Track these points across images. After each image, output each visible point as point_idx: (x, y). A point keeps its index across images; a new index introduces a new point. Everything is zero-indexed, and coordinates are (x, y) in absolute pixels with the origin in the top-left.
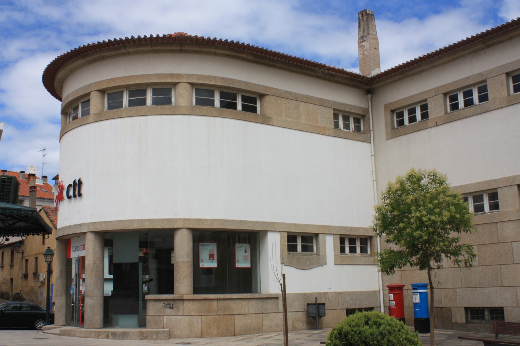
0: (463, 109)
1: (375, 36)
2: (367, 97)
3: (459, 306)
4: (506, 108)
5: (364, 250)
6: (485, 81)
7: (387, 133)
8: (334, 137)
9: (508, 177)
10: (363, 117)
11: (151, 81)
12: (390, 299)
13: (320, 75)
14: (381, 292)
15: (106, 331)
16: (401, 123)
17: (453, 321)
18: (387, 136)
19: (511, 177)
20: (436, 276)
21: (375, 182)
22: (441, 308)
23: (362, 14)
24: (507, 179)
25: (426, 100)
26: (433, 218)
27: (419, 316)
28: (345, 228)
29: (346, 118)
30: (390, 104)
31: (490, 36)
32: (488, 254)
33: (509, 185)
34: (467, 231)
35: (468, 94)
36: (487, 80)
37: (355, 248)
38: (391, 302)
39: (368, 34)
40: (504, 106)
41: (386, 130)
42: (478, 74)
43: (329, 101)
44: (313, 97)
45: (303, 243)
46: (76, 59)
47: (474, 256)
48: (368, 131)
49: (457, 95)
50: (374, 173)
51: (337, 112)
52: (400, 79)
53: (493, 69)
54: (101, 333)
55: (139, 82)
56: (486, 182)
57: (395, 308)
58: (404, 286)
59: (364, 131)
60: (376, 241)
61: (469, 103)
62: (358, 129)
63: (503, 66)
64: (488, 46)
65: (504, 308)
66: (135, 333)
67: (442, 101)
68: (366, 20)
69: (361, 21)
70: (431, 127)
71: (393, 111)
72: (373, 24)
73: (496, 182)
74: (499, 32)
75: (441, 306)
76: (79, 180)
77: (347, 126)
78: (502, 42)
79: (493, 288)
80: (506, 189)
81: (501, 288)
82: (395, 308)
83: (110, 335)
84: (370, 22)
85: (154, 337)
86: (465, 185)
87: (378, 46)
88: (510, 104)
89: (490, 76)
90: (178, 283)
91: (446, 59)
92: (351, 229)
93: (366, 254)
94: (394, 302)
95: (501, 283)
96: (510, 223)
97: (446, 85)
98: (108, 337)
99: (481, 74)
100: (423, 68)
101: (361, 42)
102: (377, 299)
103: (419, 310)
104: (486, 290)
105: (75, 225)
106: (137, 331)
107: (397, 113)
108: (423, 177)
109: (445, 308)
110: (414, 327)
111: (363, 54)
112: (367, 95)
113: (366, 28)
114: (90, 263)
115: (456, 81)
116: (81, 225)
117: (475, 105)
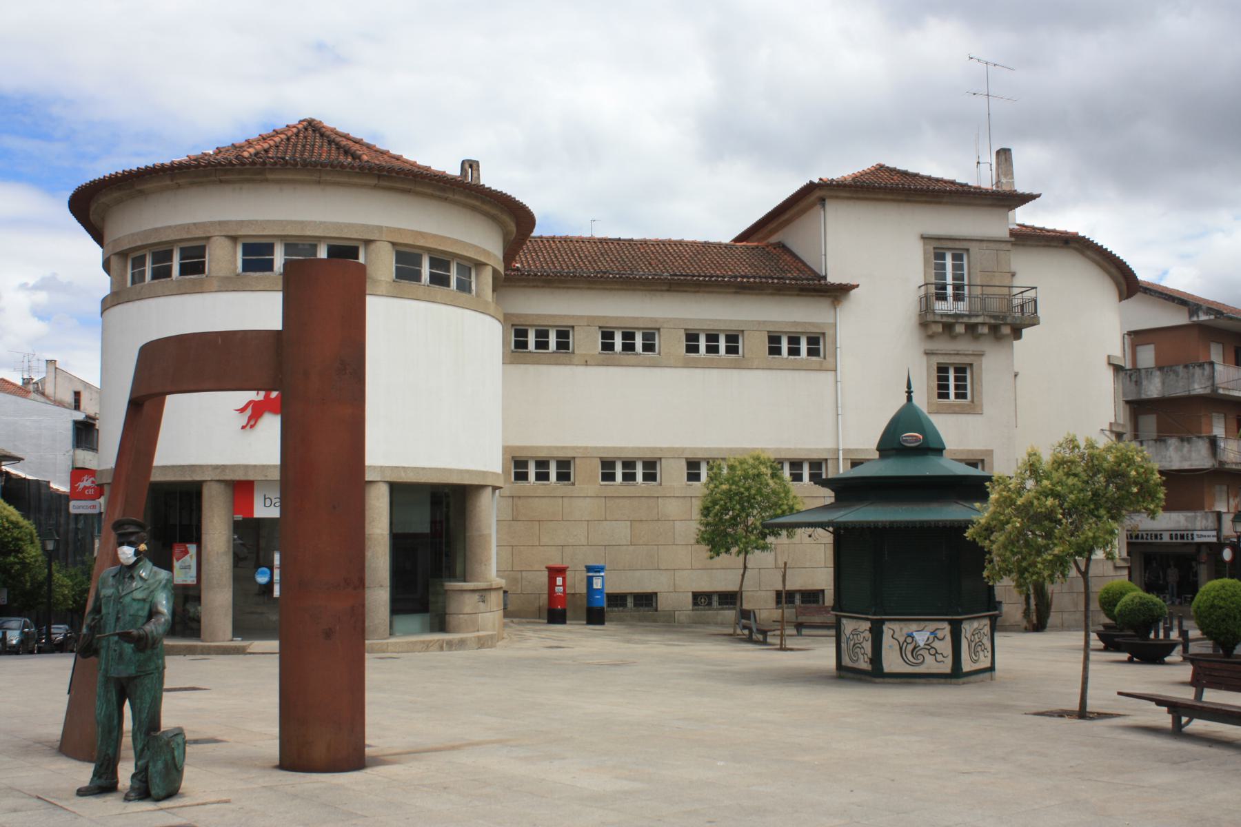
9: (678, 448)
11: (465, 253)
15: (438, 640)
16: (521, 345)
30: (512, 315)
33: (676, 456)
42: (652, 318)
53: (671, 319)
56: (647, 448)
58: (568, 567)
63: (684, 320)
65: (659, 594)
70: (577, 365)
75: (573, 592)
80: (672, 460)
83: (445, 645)
86: (621, 448)
89: (665, 326)
91: (616, 287)
94: (562, 588)
97: (604, 317)
98: (441, 649)
99: (656, 320)
100: (581, 286)
104: (638, 573)
106: (474, 637)
117: (637, 354)
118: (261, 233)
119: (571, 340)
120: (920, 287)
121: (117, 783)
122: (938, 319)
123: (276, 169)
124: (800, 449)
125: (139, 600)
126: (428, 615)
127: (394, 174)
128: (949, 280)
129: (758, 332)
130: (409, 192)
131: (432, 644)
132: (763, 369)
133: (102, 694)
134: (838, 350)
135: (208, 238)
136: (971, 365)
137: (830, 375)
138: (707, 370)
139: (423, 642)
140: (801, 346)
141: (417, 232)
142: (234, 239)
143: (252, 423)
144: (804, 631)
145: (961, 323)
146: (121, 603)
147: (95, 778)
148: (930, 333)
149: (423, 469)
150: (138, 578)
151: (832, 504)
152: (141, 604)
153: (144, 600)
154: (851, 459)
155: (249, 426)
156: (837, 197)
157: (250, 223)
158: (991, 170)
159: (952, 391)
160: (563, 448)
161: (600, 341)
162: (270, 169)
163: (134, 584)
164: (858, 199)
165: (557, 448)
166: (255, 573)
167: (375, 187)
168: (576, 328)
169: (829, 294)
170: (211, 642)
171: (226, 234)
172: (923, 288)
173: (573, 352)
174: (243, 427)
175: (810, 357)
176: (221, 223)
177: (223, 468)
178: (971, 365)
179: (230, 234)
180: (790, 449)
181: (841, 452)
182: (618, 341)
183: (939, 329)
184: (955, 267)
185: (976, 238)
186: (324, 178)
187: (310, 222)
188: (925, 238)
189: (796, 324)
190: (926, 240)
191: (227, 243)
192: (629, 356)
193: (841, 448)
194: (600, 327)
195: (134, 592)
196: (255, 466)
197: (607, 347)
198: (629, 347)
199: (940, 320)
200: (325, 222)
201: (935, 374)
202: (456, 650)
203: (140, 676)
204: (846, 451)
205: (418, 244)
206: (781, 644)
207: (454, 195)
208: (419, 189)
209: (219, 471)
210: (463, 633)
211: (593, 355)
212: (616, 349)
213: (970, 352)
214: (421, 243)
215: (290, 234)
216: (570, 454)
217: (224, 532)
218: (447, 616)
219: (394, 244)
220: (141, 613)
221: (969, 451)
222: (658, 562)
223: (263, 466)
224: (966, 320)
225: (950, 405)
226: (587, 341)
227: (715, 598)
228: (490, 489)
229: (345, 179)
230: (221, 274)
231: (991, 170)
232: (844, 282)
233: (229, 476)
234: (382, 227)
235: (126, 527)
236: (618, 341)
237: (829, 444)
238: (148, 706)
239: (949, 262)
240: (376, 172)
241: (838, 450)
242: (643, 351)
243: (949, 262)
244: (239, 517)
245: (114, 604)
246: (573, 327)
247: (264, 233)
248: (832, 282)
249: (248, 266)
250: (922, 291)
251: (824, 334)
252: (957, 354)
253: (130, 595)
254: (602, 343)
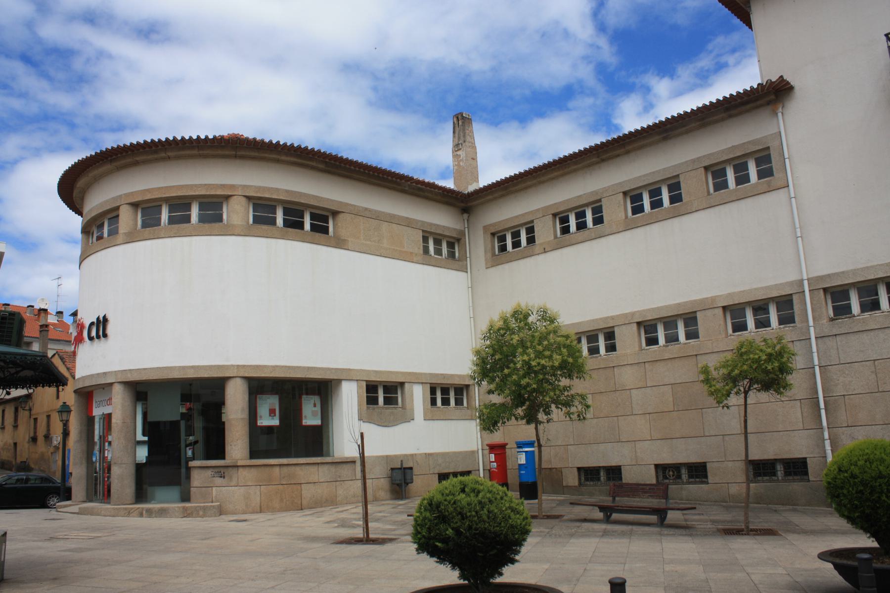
0: (575, 233)
1: (472, 144)
2: (463, 217)
3: (570, 466)
4: (623, 232)
5: (459, 402)
6: (600, 201)
7: (486, 260)
8: (424, 264)
9: (626, 314)
10: (458, 240)
11: (197, 193)
12: (491, 460)
13: (407, 189)
14: (480, 452)
15: (139, 508)
16: (503, 248)
17: (564, 484)
18: (486, 264)
19: (629, 313)
20: (545, 431)
21: (472, 319)
22: (550, 469)
23: (458, 118)
24: (625, 315)
25: (532, 221)
26: (543, 362)
27: (525, 480)
28: (437, 375)
29: (438, 242)
30: (491, 225)
31: (605, 149)
32: (603, 405)
34: (580, 378)
35: (581, 215)
36: (602, 199)
37: (449, 399)
38: (492, 464)
39: (464, 142)
40: (621, 230)
41: (485, 256)
43: (417, 221)
44: (398, 216)
45: (613, 343)
46: (101, 164)
47: (588, 407)
48: (464, 258)
49: (568, 216)
50: (471, 308)
51: (427, 235)
52: (502, 196)
53: (609, 187)
54: (133, 511)
55: (182, 194)
56: (601, 319)
57: (496, 470)
58: (507, 444)
59: (459, 257)
60: (474, 391)
61: (581, 226)
62: (452, 255)
63: (620, 183)
64: (603, 160)
65: (622, 467)
66: (176, 509)
67: (551, 223)
68: (462, 125)
69: (457, 125)
70: (538, 254)
71: (493, 234)
72: (470, 129)
73: (613, 319)
74: (615, 145)
75: (550, 467)
76: (104, 317)
77: (438, 252)
78: (618, 156)
79: (609, 444)
80: (624, 327)
81: (618, 443)
82: (496, 470)
83: (144, 512)
84: (467, 128)
85: (201, 513)
87: (476, 156)
88: (627, 228)
90: (231, 445)
91: (556, 174)
92: (444, 376)
93: (461, 407)
94: (495, 464)
95: (618, 437)
96: (628, 367)
97: (555, 204)
98: (141, 515)
99: (595, 193)
100: (529, 183)
101: (456, 151)
102: (475, 460)
103: (524, 472)
104: (602, 447)
105: (98, 374)
106: (177, 507)
107: (498, 237)
108: (530, 313)
109: (554, 470)
110: (519, 493)
111: (458, 165)
112: (462, 214)
113: (462, 134)
115: (567, 200)
116: (106, 374)
117: (589, 229)
124: (756, 289)
129: (694, 171)
132: (704, 209)
134: (787, 161)
138: (648, 227)
140: (750, 171)
144: (615, 516)
169: (759, 103)
180: (743, 291)
181: (806, 283)
189: (734, 148)
193: (805, 277)
212: (571, 231)
222: (619, 433)
226: (546, 231)
227: (684, 471)
236: (573, 223)
237: (793, 277)
241: (802, 281)
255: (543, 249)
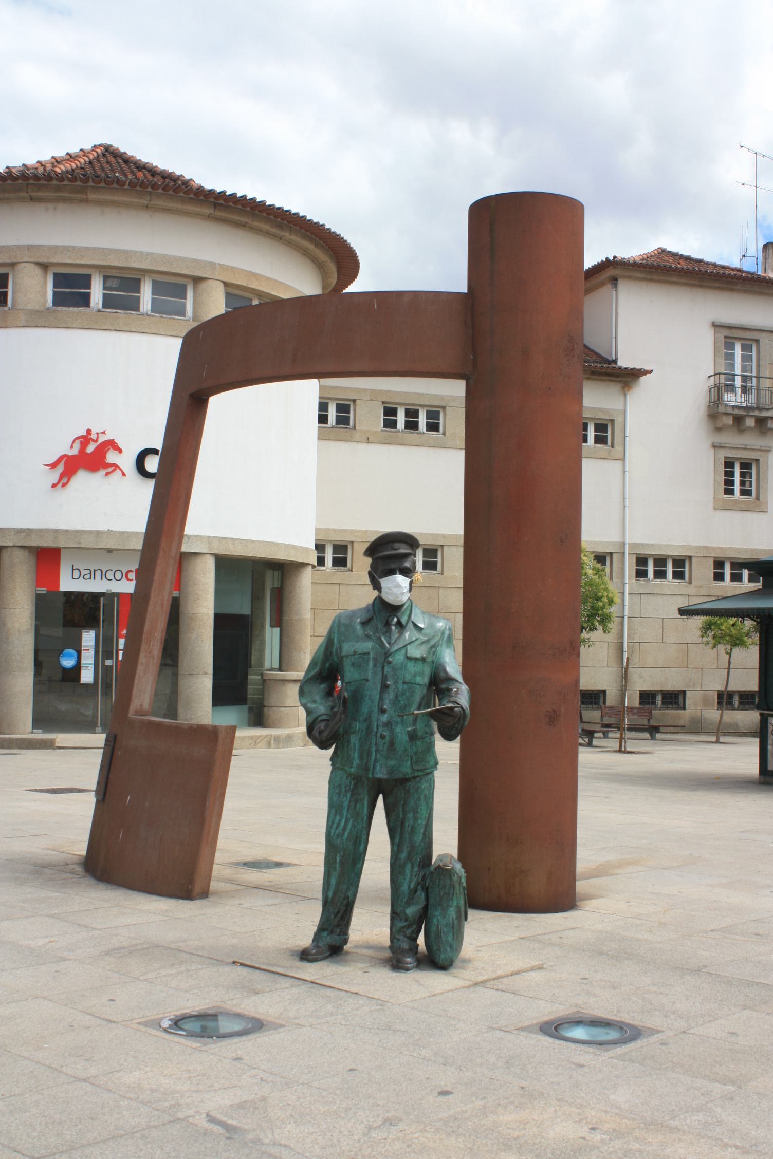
56: (430, 534)
61: (412, 425)
73: (444, 537)
83: (272, 741)
114: (210, 613)
115: (405, 393)
117: (420, 433)
118: (78, 262)
119: (351, 415)
120: (709, 377)
121: (346, 941)
122: (730, 410)
123: (101, 187)
125: (416, 659)
126: (245, 707)
127: (231, 204)
128: (738, 370)
130: (244, 226)
131: (260, 739)
133: (346, 803)
134: (627, 439)
135: (13, 265)
136: (757, 461)
137: (618, 465)
139: (251, 738)
141: (250, 272)
142: (44, 267)
143: (64, 480)
145: (752, 416)
146: (390, 663)
147: (325, 934)
148: (720, 425)
149: (252, 541)
150: (410, 625)
151: (759, 590)
152: (419, 667)
153: (423, 660)
154: (636, 554)
155: (60, 485)
156: (630, 278)
157: (66, 249)
158: (757, 264)
159: (737, 487)
160: (341, 531)
161: (382, 417)
162: (93, 187)
163: (407, 635)
164: (651, 280)
165: (334, 531)
166: (59, 656)
167: (209, 217)
168: (358, 402)
170: (9, 734)
171: (36, 260)
172: (712, 378)
173: (354, 428)
174: (54, 486)
175: (597, 445)
176: (30, 248)
177: (29, 532)
178: (757, 461)
179: (40, 261)
181: (627, 546)
182: (401, 418)
183: (729, 421)
184: (744, 358)
185: (766, 329)
186: (154, 203)
187: (136, 252)
188: (716, 326)
190: (717, 329)
191: (38, 271)
192: (414, 435)
193: (627, 542)
194: (383, 403)
195: (408, 646)
196: (67, 531)
197: (390, 424)
198: (412, 425)
199: (732, 412)
200: (152, 254)
201: (722, 468)
202: (283, 747)
203: (414, 778)
204: (633, 545)
205: (252, 287)
206: (621, 746)
207: (290, 235)
208: (256, 224)
209: (23, 535)
210: (284, 728)
211: (376, 432)
213: (758, 448)
214: (254, 285)
215: (113, 264)
216: (348, 538)
217: (27, 607)
218: (266, 709)
219: (226, 284)
220: (419, 679)
221: (753, 550)
223: (77, 531)
224: (756, 413)
225: (736, 502)
228: (311, 567)
229: (179, 206)
230: (29, 307)
231: (757, 264)
232: (638, 367)
233: (36, 542)
234: (215, 263)
235: (397, 545)
236: (401, 418)
237: (615, 537)
238: (424, 823)
239: (738, 352)
240: (212, 200)
241: (624, 544)
242: (427, 430)
243: (738, 352)
244: (43, 590)
245: (375, 665)
246: (354, 401)
247: (82, 262)
248: (625, 366)
249: (59, 300)
250: (711, 382)
251: (612, 421)
252: (745, 449)
253: (403, 651)
254: (384, 419)
255: (366, 439)
